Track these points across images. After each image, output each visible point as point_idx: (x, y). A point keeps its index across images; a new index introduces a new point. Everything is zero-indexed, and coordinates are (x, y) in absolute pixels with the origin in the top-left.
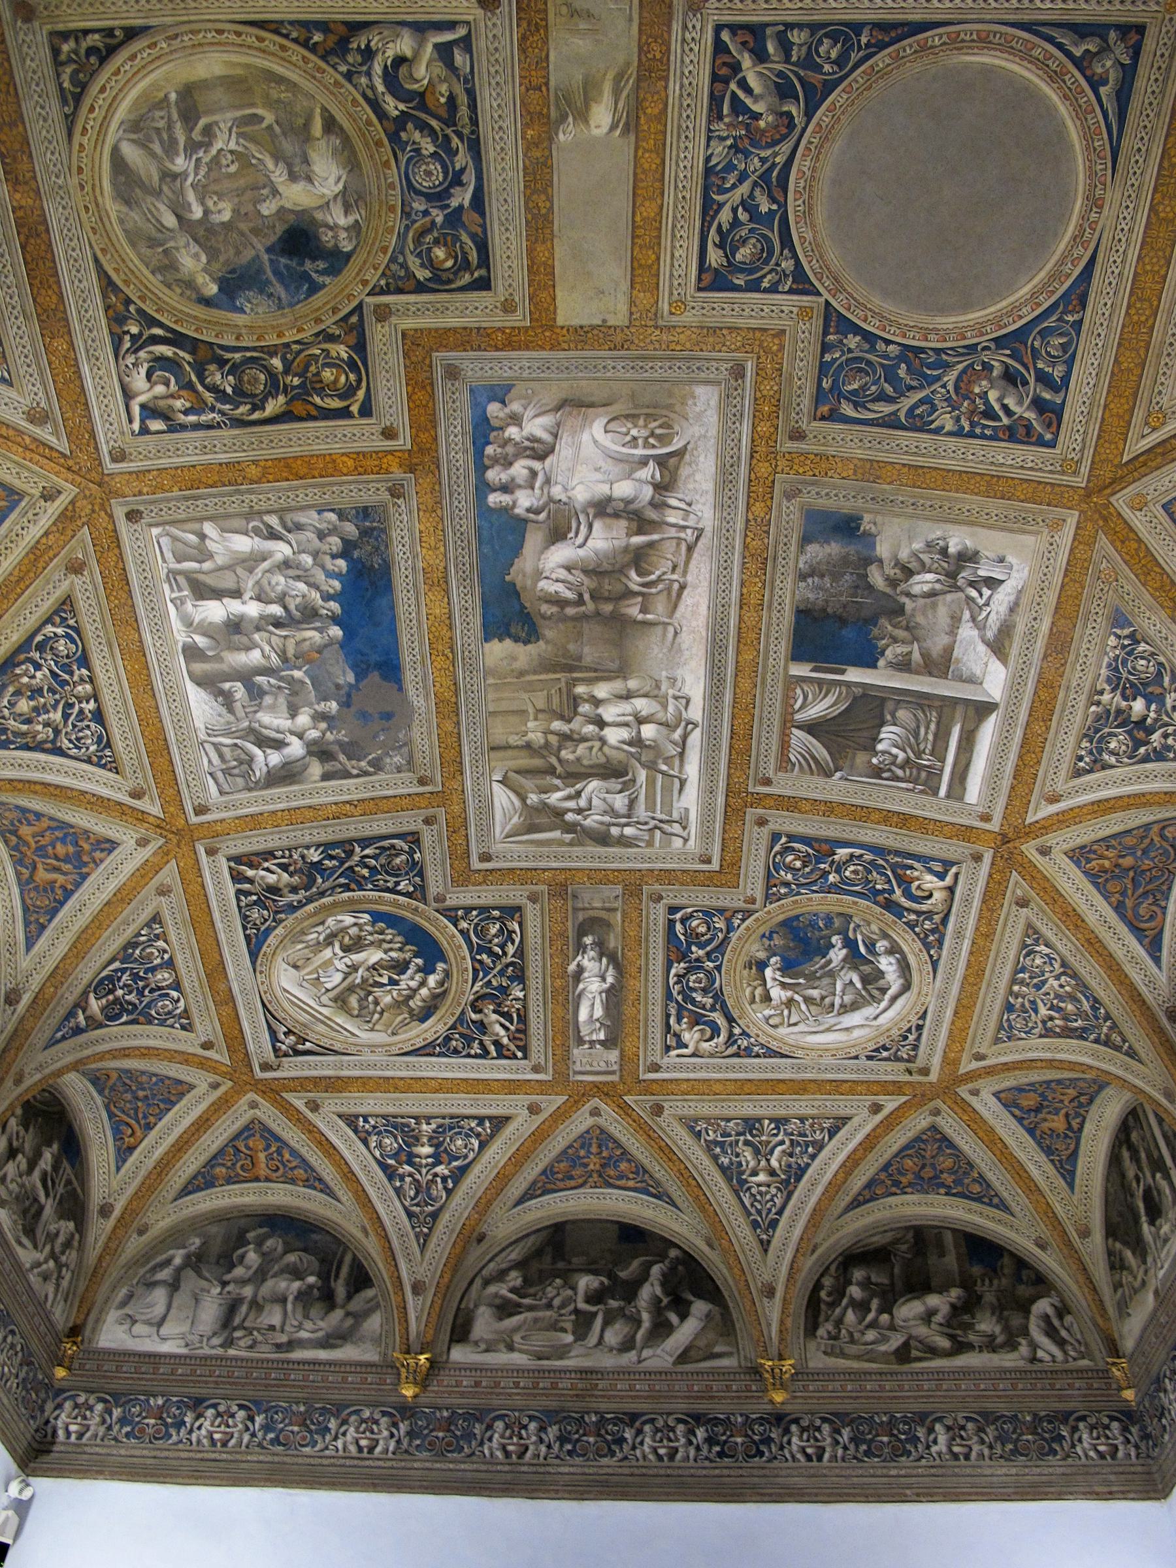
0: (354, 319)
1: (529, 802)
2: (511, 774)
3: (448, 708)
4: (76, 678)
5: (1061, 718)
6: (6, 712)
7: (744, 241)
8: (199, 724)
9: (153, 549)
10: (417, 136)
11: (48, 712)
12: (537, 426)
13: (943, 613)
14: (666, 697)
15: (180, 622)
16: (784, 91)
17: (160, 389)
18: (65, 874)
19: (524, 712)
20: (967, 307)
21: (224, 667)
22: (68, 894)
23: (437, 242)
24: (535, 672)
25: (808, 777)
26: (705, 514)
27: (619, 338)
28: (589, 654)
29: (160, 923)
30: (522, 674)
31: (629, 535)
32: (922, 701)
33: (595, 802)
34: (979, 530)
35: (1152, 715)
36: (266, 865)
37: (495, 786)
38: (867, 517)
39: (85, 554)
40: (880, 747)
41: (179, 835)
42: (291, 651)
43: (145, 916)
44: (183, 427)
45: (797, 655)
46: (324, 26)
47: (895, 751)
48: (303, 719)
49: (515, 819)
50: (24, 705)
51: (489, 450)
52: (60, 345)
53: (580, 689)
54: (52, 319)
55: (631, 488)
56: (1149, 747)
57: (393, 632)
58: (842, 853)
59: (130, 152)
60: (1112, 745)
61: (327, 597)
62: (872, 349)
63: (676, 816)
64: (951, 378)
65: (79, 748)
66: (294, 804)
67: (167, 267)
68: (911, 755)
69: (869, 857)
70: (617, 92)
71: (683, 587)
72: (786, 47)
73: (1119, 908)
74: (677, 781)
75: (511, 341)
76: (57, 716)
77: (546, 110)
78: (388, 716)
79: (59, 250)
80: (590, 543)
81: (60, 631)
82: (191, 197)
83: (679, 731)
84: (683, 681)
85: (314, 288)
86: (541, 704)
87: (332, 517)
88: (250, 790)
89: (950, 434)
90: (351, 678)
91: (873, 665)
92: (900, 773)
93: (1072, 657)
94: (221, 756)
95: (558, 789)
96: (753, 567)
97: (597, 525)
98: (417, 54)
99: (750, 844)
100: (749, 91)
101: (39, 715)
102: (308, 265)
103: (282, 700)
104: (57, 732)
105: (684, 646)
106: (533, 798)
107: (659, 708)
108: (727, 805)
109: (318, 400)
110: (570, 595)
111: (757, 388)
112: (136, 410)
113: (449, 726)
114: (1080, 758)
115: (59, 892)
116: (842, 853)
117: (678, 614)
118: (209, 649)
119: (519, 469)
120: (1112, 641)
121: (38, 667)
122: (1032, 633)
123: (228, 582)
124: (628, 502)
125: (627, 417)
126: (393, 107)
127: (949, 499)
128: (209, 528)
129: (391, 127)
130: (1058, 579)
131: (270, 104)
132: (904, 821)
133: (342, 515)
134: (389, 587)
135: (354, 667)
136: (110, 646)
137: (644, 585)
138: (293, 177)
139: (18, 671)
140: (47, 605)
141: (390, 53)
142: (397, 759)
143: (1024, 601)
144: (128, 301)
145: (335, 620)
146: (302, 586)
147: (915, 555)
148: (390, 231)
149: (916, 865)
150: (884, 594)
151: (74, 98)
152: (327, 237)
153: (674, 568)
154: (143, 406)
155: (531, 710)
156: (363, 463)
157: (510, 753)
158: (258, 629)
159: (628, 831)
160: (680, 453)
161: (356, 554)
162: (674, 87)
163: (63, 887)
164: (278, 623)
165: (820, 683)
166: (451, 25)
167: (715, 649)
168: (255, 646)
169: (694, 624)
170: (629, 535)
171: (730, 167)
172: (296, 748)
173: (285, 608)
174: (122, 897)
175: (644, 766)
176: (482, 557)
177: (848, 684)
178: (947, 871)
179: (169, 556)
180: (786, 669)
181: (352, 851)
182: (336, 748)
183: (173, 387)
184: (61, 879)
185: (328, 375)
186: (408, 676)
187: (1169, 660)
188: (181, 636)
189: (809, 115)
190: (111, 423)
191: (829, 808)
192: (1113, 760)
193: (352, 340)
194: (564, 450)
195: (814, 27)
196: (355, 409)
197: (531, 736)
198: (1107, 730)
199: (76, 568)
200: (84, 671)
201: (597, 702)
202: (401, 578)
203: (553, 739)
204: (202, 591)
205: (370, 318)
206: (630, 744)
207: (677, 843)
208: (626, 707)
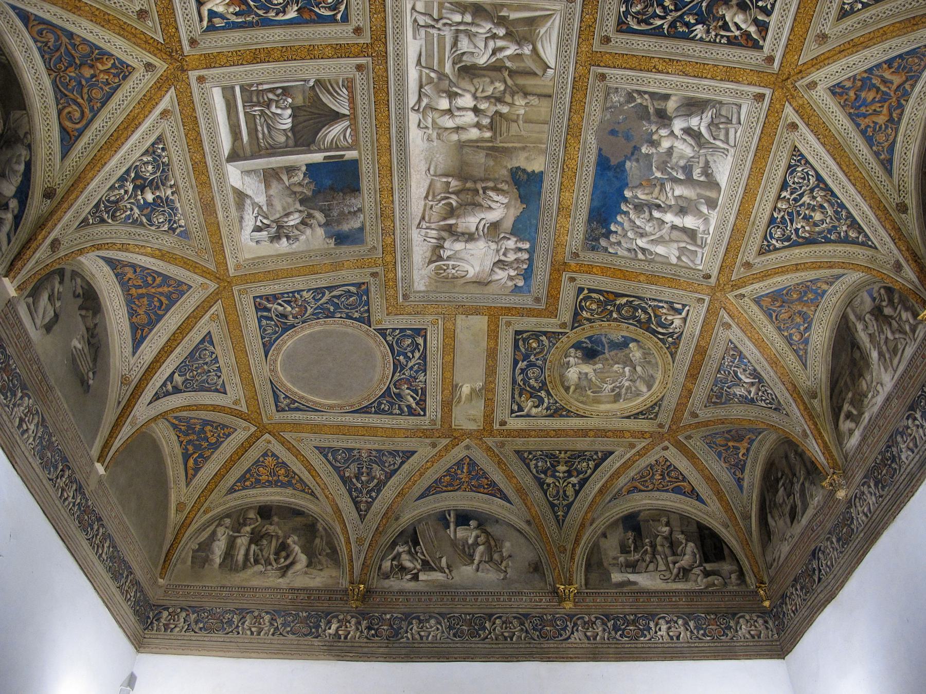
0: (576, 325)
1: (531, 47)
2: (539, 73)
3: (573, 131)
4: (782, 213)
5: (187, 169)
6: (828, 220)
7: (408, 346)
8: (730, 158)
9: (706, 260)
10: (536, 385)
11: (809, 204)
12: (501, 275)
13: (278, 206)
14: (433, 128)
15: (711, 224)
16: (399, 396)
17: (670, 318)
18: (882, 77)
19: (525, 122)
20: (310, 334)
21: (699, 191)
22: (889, 62)
23: (535, 349)
24: (515, 148)
25: (332, 76)
26: (416, 236)
27: (461, 310)
28: (481, 158)
29: (842, 8)
30: (524, 148)
31: (456, 224)
32: (273, 150)
33: (481, 45)
34: (274, 253)
35: (140, 197)
36: (737, 33)
37: (552, 65)
38: (332, 245)
39: (739, 269)
40: (289, 111)
41: (784, 82)
42: (657, 189)
43: (849, 22)
44: (666, 302)
45: (355, 163)
46: (561, 416)
47: (279, 111)
48: (666, 144)
49: (542, 31)
50: (818, 216)
51: (525, 266)
52: (703, 343)
53: (488, 135)
54: (701, 352)
55: (453, 247)
56: (130, 180)
57: (595, 186)
58: (292, 14)
59: (644, 389)
60: (150, 167)
61: (626, 213)
62: (347, 314)
63: (422, 31)
64: (310, 311)
65: (807, 173)
66: (696, 81)
67: (646, 354)
68: (267, 112)
69: (272, 14)
70: (460, 397)
71: (426, 197)
72: (400, 408)
73: (71, 35)
74: (423, 64)
75: (509, 310)
76: (806, 199)
77: (487, 392)
78: (613, 132)
79: (686, 368)
80: (478, 220)
81: (774, 242)
82: (627, 374)
83: (423, 104)
84: (423, 140)
85: (590, 338)
86: (515, 125)
87: (610, 250)
88: (721, 103)
89: (303, 291)
90: (628, 164)
91: (308, 166)
92: (271, 96)
93: (199, 204)
94: (727, 134)
95: (508, 57)
96: (388, 211)
97: (473, 229)
98: (531, 409)
99: (364, 8)
100: (412, 396)
101: (814, 206)
102: (590, 346)
103: (674, 160)
104: (812, 190)
105: (423, 162)
106: (527, 50)
107: (438, 121)
108: (385, 44)
109: (602, 298)
110: (491, 193)
111: (396, 291)
112: (684, 314)
113: (576, 119)
114: (163, 149)
115: (896, 65)
116: (292, 14)
117: (428, 182)
118: (702, 203)
119: (511, 257)
120: (182, 223)
121: (797, 230)
122: (226, 209)
123: (675, 234)
124: (457, 240)
125: (457, 278)
126: (543, 394)
127: (295, 264)
128: (674, 260)
129: (545, 388)
130: (225, 240)
131: (588, 396)
132: (257, 56)
133: (606, 249)
134: (591, 211)
135: (624, 171)
136: (754, 223)
137: (448, 198)
138: (586, 374)
139: (807, 235)
140: (772, 256)
141: (540, 409)
142: (615, 99)
143: (237, 224)
144: (667, 348)
145: (626, 200)
146: (638, 223)
147: (303, 233)
148: (553, 354)
149: (234, 19)
150: (313, 209)
151: (658, 404)
152: (579, 354)
153: (431, 207)
154: (680, 314)
155: (521, 122)
156: (589, 269)
157: (538, 91)
158: (670, 206)
159: (457, 18)
160: (431, 262)
161: (604, 231)
162: (439, 398)
163: (890, 67)
164: (658, 207)
165: (338, 148)
166: (517, 416)
167: (404, 162)
168: (677, 198)
169: (418, 176)
170: (456, 224)
171: (417, 372)
172: (678, 125)
173: (651, 214)
174: (854, 46)
175: (447, 77)
176: (538, 220)
177: (320, 150)
178: (210, 21)
179: (699, 255)
180: (360, 153)
181: (670, 26)
182: (653, 118)
183: (663, 318)
184: (887, 75)
185: (594, 306)
186: (593, 158)
187: (150, 230)
188: (714, 217)
189: (389, 388)
190: (697, 314)
191: (312, 53)
192: (145, 159)
193: (579, 317)
194: (488, 264)
195: (391, 414)
196: (586, 291)
197: (523, 103)
198: (158, 174)
199: (748, 265)
200: (775, 215)
201: (478, 125)
202: (583, 214)
203: (508, 99)
204: (691, 234)
205: (569, 324)
206: (456, 94)
207: (420, 7)
208: (459, 121)
